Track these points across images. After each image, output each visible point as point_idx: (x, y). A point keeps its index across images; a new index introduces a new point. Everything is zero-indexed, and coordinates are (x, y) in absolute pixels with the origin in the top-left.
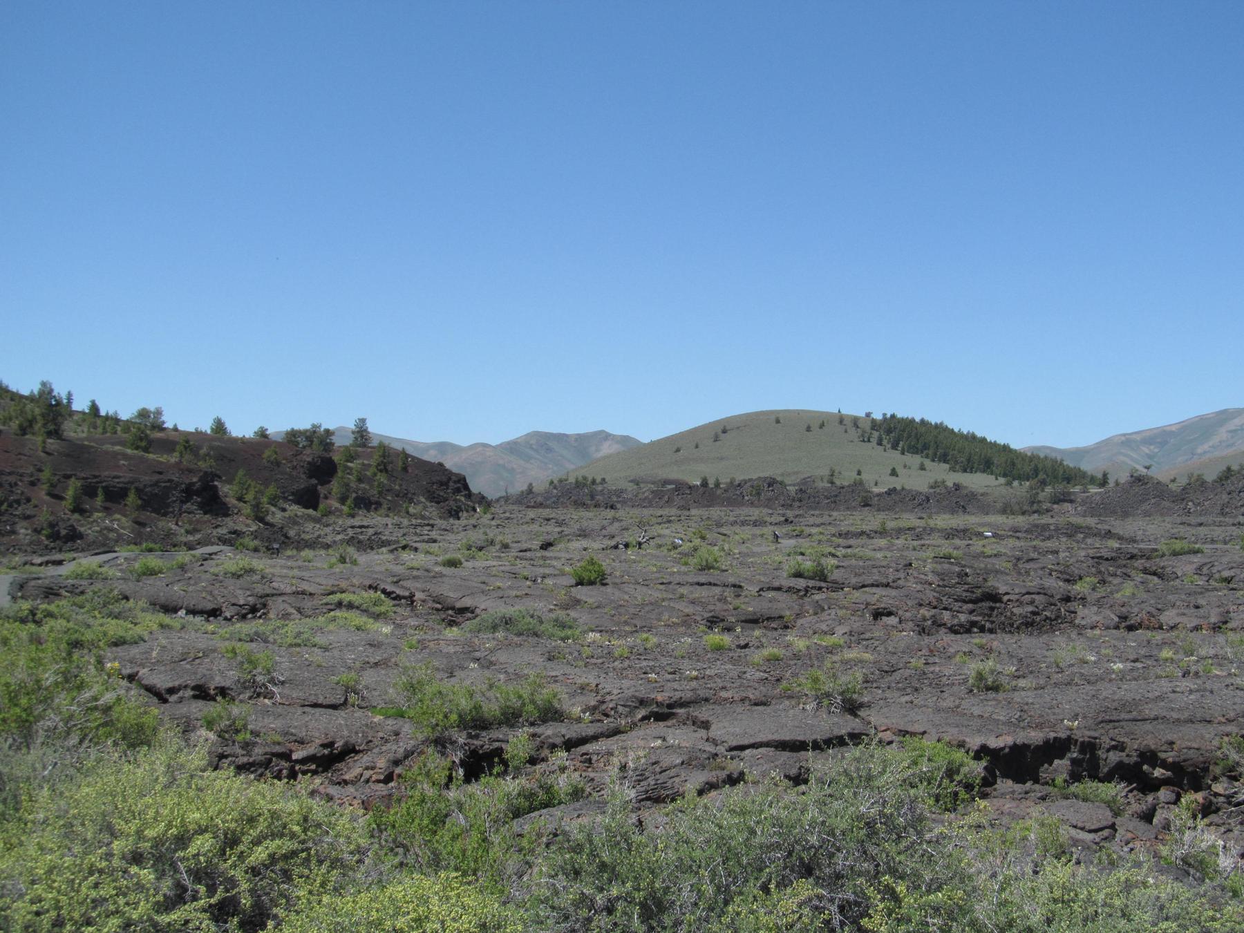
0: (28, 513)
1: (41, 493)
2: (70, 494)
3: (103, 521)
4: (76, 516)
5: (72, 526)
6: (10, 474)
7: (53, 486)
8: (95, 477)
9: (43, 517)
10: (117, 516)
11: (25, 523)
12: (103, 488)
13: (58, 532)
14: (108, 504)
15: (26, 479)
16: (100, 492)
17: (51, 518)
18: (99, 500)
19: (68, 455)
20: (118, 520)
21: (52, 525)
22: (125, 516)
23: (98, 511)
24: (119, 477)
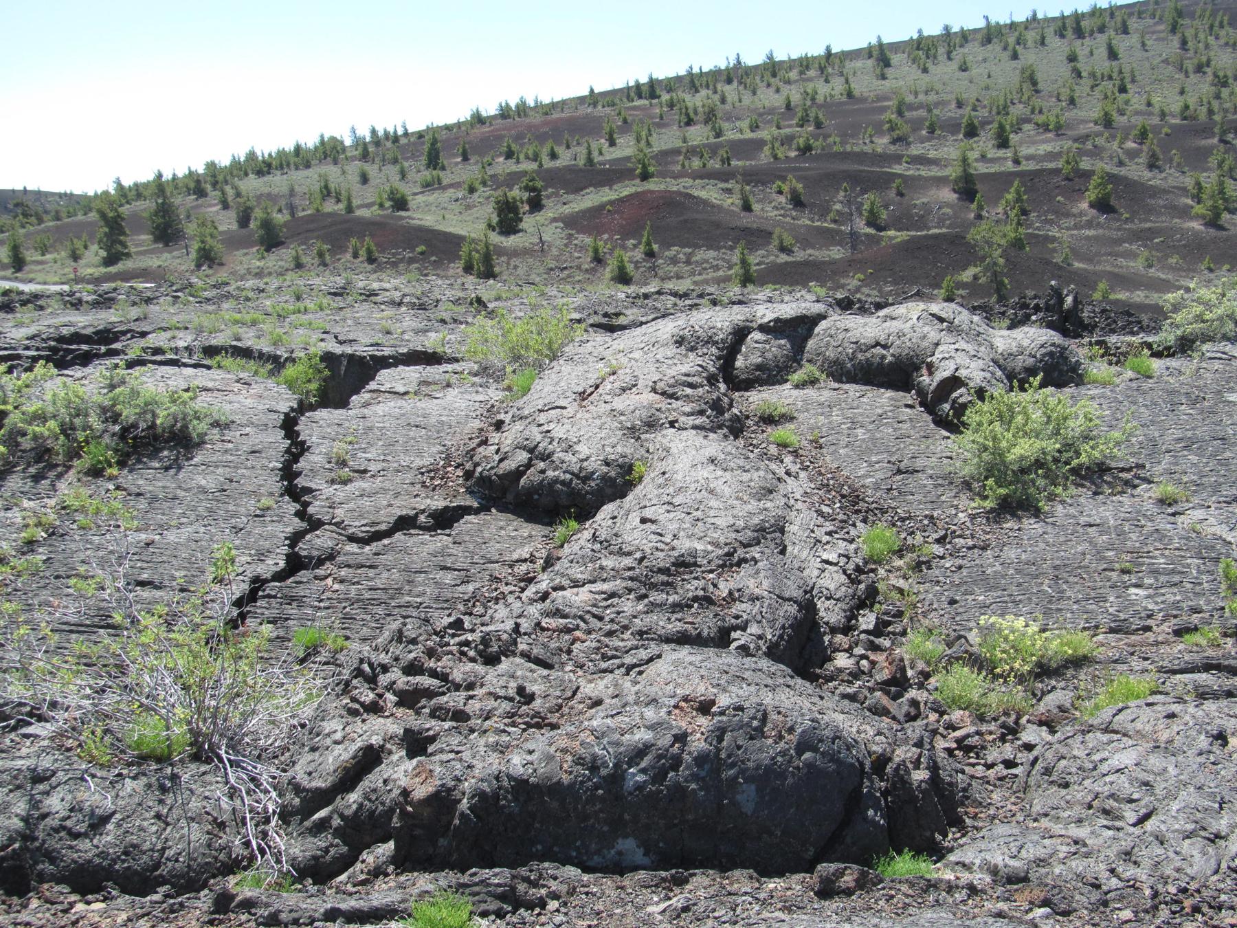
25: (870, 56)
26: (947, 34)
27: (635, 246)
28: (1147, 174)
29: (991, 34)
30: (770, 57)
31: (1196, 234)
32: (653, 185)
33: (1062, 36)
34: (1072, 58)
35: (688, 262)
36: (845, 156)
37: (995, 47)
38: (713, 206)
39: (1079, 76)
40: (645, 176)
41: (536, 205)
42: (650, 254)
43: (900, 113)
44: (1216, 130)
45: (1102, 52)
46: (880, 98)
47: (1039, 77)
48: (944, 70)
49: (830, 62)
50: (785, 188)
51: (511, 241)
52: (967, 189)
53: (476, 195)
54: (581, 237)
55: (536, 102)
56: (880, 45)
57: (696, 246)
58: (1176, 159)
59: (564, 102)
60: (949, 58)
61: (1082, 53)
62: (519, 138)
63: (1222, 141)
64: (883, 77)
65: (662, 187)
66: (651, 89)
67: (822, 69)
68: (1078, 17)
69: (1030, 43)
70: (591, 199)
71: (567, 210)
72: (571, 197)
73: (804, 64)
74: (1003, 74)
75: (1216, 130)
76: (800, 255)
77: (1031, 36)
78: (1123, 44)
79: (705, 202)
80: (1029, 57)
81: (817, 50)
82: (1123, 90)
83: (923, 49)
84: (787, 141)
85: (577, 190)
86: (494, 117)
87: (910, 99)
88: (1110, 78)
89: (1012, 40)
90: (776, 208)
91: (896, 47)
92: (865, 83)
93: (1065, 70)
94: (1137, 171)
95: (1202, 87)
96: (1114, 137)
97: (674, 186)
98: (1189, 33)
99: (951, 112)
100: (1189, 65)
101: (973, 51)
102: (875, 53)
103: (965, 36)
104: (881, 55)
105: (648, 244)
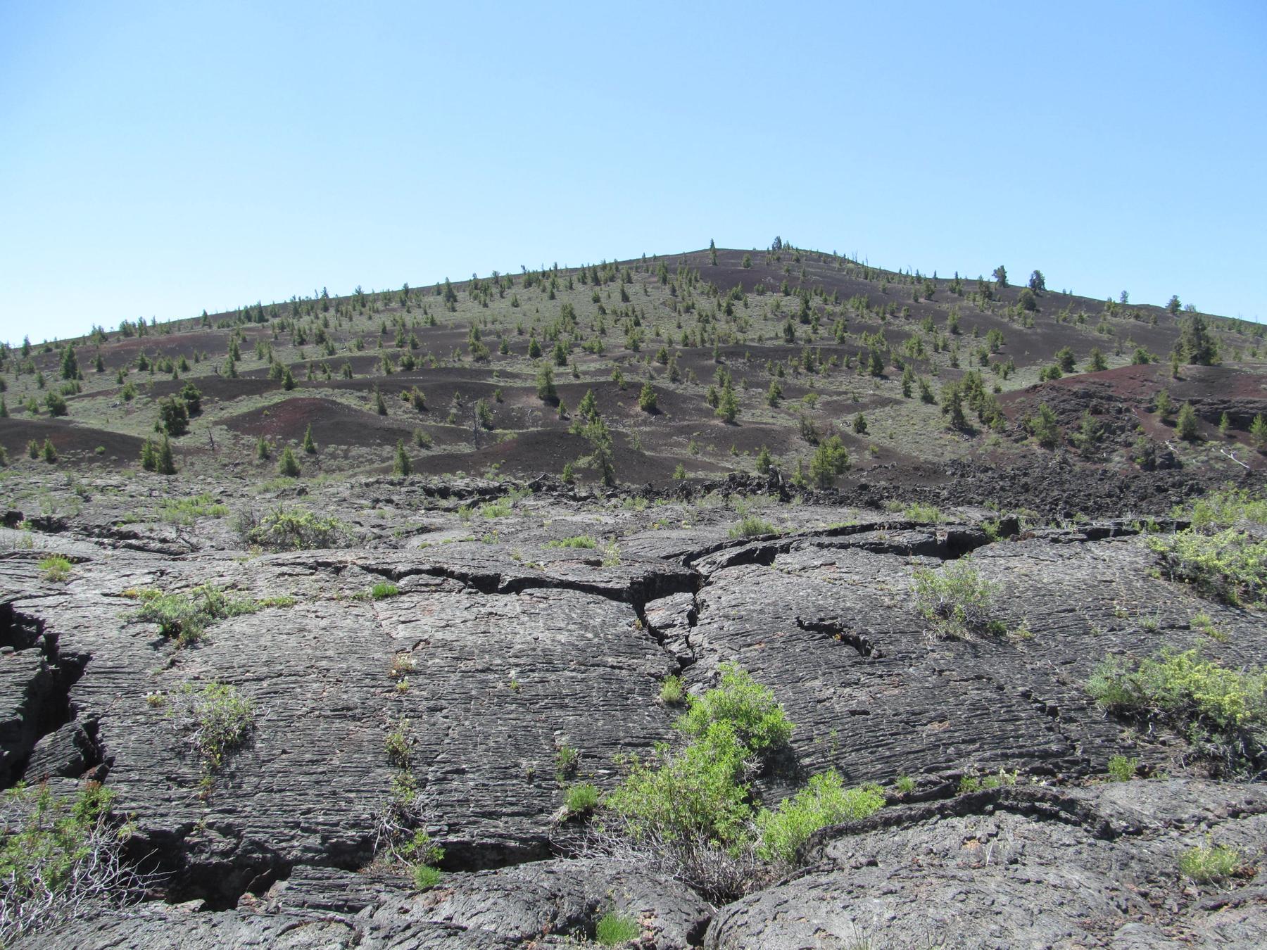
0: (1131, 440)
1: (1156, 420)
2: (1181, 420)
3: (1218, 450)
4: (1186, 444)
5: (1170, 454)
6: (1125, 400)
7: (1171, 412)
8: (1224, 402)
9: (1140, 443)
10: (1239, 445)
11: (1122, 451)
12: (1229, 414)
13: (1153, 461)
14: (1234, 432)
15: (1144, 405)
16: (1224, 418)
17: (1148, 446)
18: (1222, 428)
19: (1201, 380)
20: (1239, 449)
21: (1147, 454)
22: (1250, 445)
23: (1216, 438)
24: (1255, 402)
25: (439, 294)
26: (496, 279)
27: (297, 445)
28: (672, 386)
29: (531, 280)
30: (359, 292)
31: (720, 429)
32: (298, 393)
33: (584, 283)
34: (596, 300)
35: (346, 457)
36: (440, 371)
37: (534, 290)
38: (355, 411)
39: (604, 312)
40: (290, 386)
41: (195, 411)
42: (311, 451)
43: (477, 338)
44: (714, 354)
45: (617, 296)
46: (458, 326)
47: (576, 313)
48: (500, 306)
49: (407, 296)
50: (411, 396)
51: (181, 442)
52: (551, 397)
53: (133, 402)
54: (246, 437)
55: (154, 322)
56: (448, 284)
57: (351, 444)
58: (691, 375)
59: (180, 322)
60: (502, 297)
61: (603, 296)
62: (148, 352)
63: (718, 362)
64: (454, 310)
65: (306, 395)
66: (259, 314)
67: (403, 303)
68: (594, 269)
69: (561, 288)
70: (245, 405)
71: (225, 414)
72: (227, 403)
73: (387, 297)
74: (550, 312)
75: (714, 354)
76: (437, 450)
77: (561, 282)
78: (631, 290)
79: (348, 407)
80: (564, 298)
81: (397, 286)
82: (637, 324)
83: (479, 288)
84: (394, 357)
85: (231, 397)
86: (113, 334)
87: (481, 327)
88: (627, 315)
89: (548, 284)
90: (405, 412)
91: (461, 286)
92: (442, 315)
93: (594, 308)
94: (664, 382)
95: (691, 325)
96: (643, 358)
97: (319, 394)
98: (676, 284)
99: (513, 338)
100: (681, 307)
101: (518, 291)
102: (444, 291)
103: (511, 280)
104: (449, 292)
105: (310, 442)
